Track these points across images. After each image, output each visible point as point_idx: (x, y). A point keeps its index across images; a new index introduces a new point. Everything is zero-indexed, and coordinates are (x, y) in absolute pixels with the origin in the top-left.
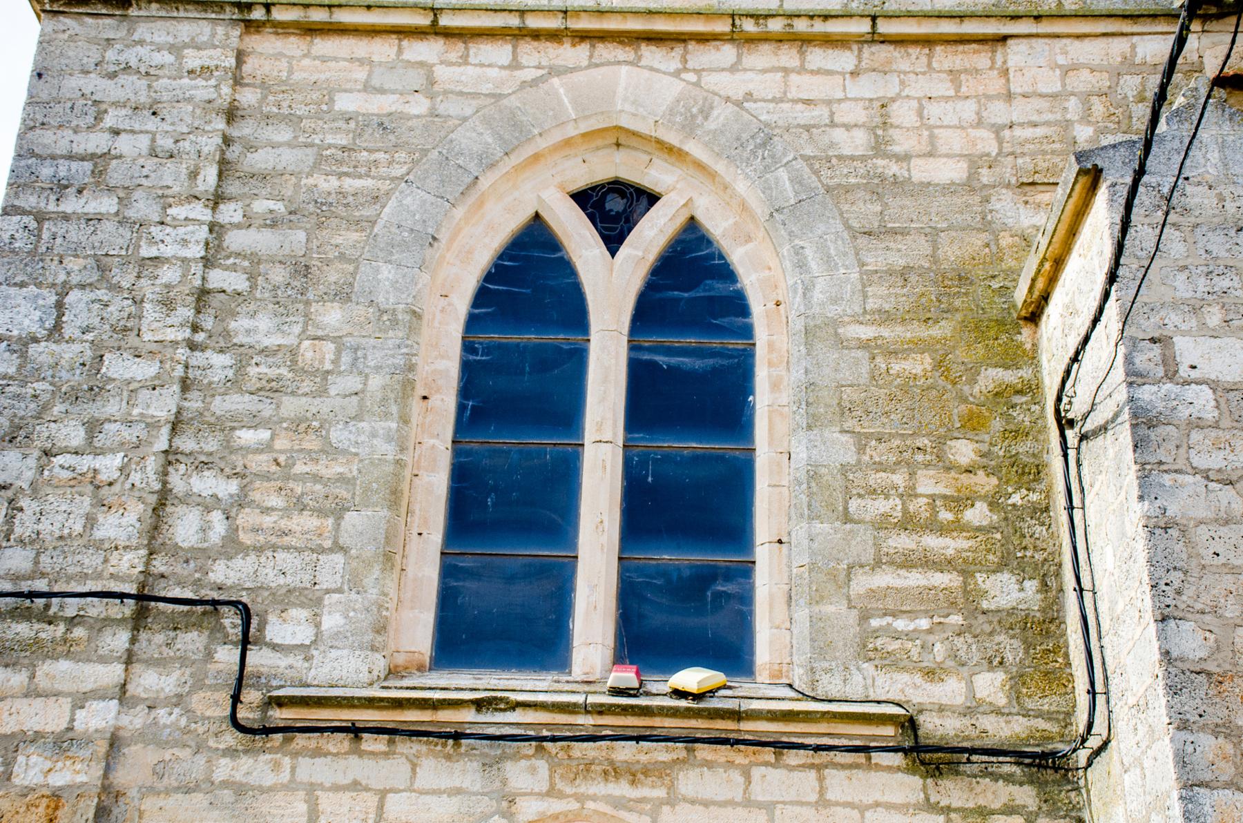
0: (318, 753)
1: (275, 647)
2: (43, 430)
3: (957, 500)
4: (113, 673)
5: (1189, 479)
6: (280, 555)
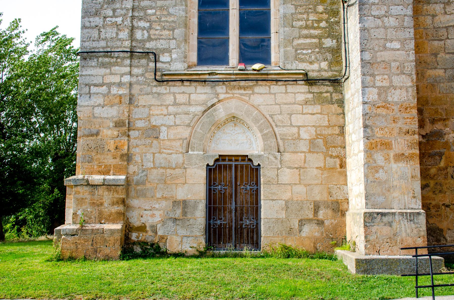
0: (174, 86)
1: (162, 62)
2: (103, 12)
3: (318, 21)
4: (128, 69)
5: (370, 18)
6: (161, 41)
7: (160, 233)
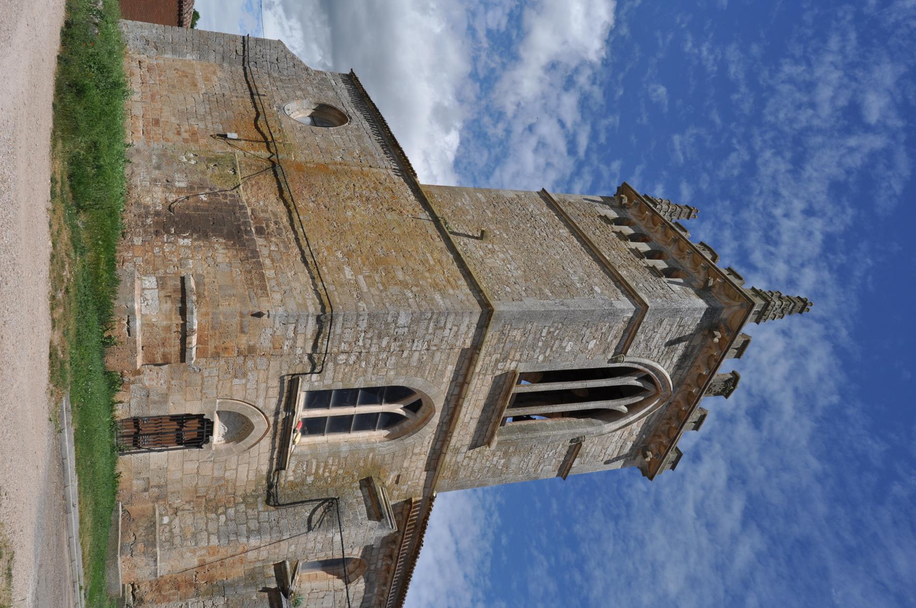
7: (132, 386)
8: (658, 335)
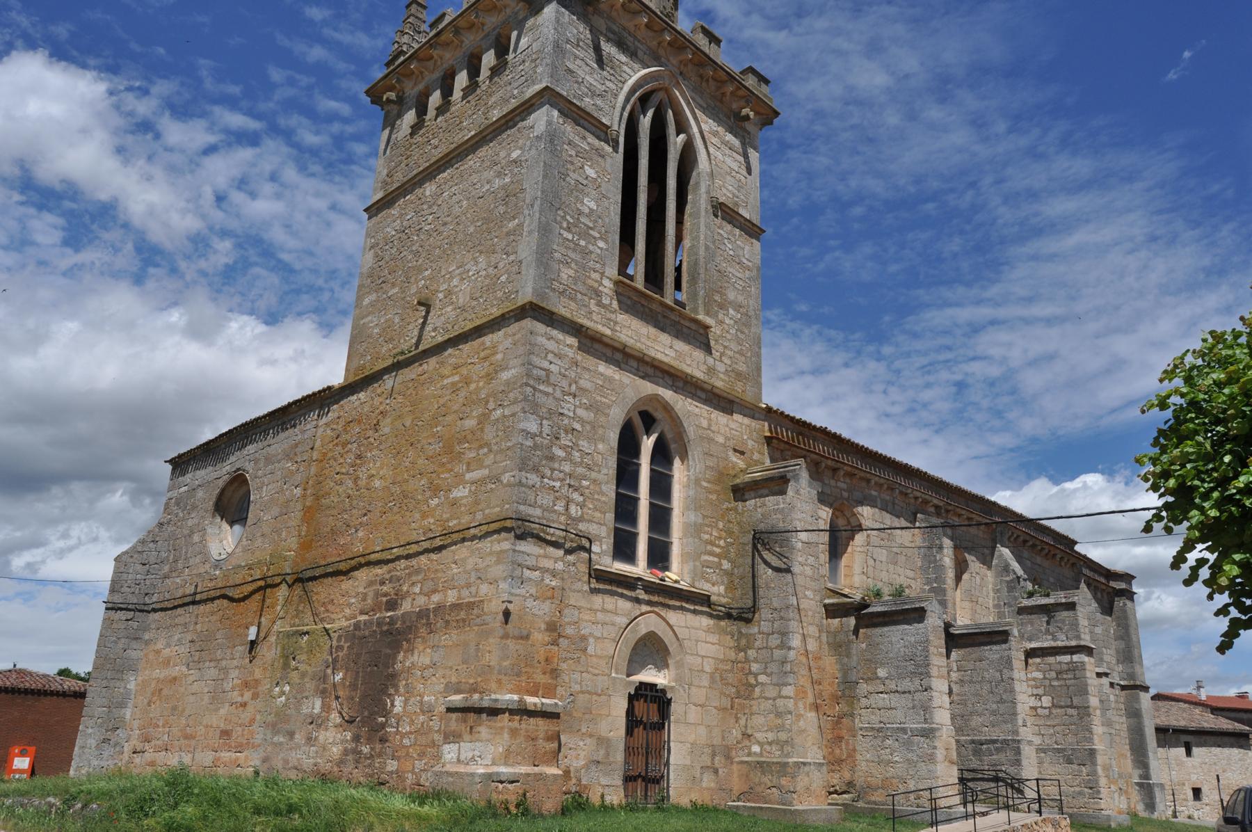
7: (584, 782)
8: (587, 77)
